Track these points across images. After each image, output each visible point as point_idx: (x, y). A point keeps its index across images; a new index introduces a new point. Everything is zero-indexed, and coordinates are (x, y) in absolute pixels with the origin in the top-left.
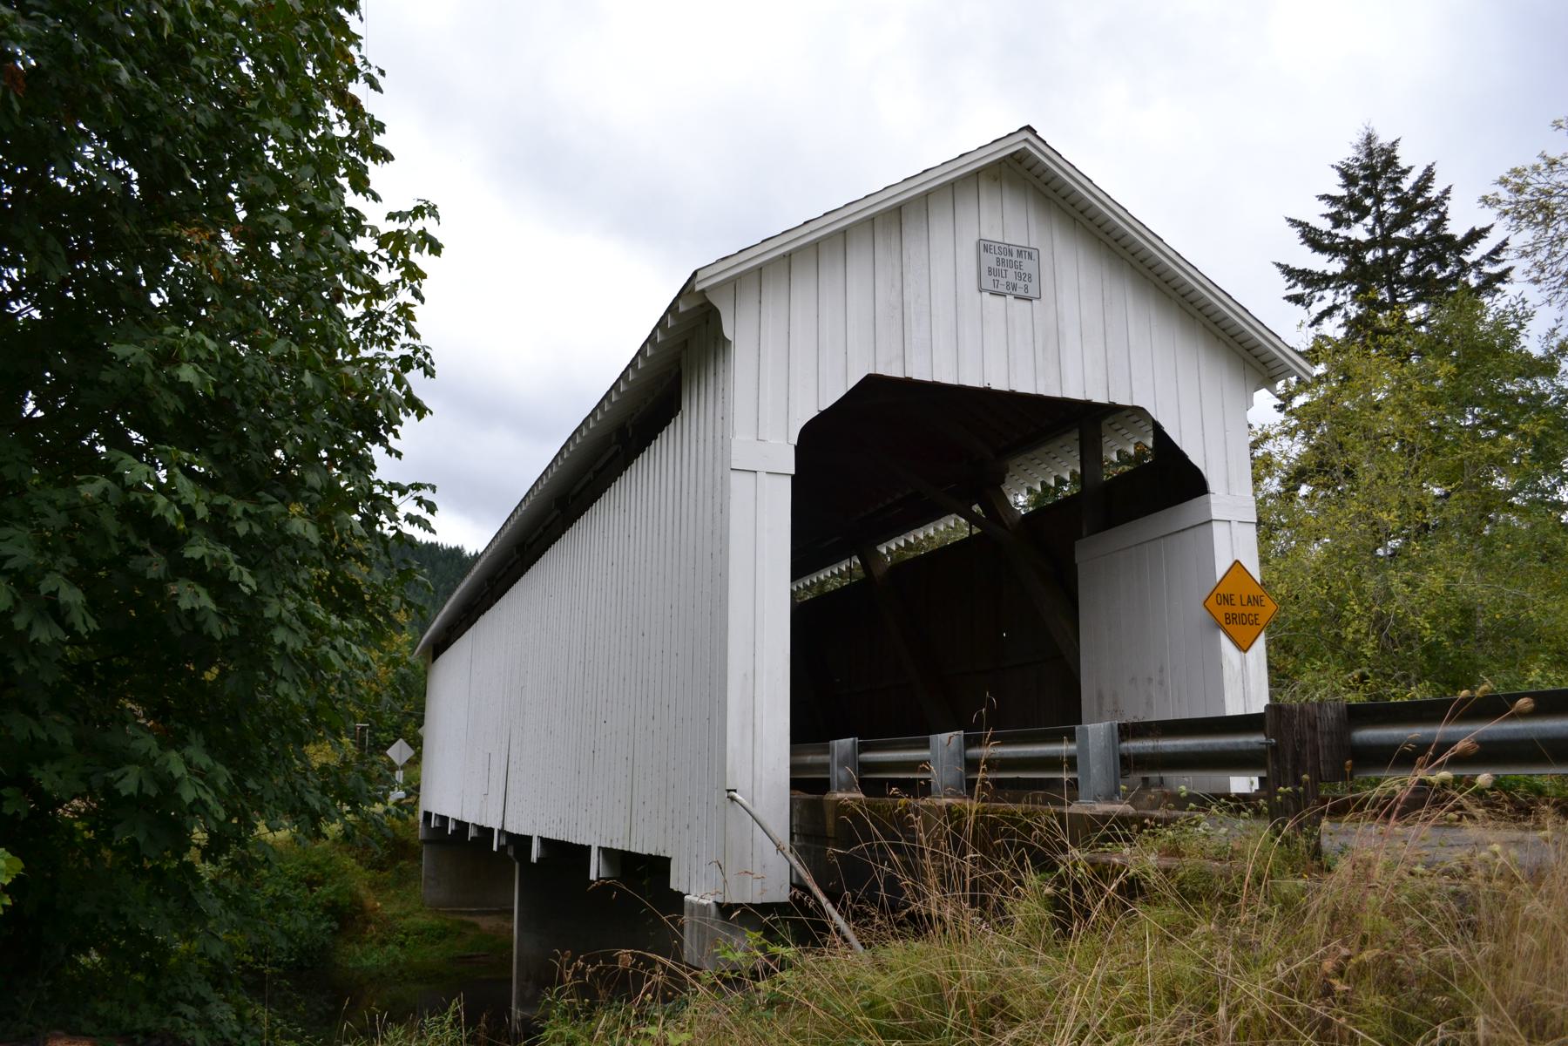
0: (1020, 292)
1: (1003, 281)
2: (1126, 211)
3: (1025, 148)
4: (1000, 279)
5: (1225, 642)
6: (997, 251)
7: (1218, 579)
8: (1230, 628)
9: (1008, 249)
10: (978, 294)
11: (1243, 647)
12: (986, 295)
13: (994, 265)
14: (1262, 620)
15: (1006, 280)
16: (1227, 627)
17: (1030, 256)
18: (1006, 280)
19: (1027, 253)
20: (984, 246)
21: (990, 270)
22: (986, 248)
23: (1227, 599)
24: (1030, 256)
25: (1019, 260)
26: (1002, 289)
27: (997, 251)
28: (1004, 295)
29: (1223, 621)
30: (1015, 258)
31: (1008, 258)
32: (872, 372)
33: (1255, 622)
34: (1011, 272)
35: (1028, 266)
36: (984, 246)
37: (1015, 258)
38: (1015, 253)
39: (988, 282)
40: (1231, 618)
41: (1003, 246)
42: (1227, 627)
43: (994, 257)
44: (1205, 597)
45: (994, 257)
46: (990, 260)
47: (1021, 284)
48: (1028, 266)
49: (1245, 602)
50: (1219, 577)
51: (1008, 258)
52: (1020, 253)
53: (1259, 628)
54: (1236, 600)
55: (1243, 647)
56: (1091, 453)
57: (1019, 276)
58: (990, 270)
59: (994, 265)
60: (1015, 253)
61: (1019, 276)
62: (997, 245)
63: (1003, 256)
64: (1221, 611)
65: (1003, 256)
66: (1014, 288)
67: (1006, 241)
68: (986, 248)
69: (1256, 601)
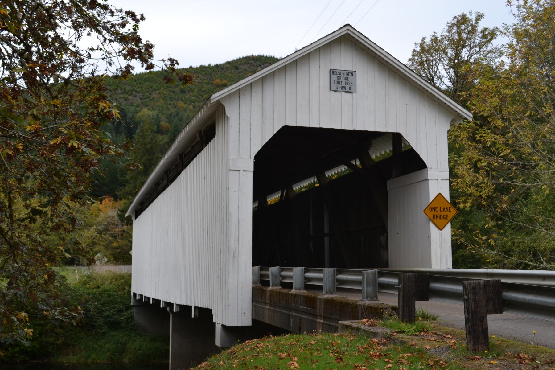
0: (347, 90)
1: (340, 86)
2: (391, 55)
3: (347, 33)
4: (339, 85)
5: (432, 226)
6: (338, 73)
7: (430, 201)
8: (434, 220)
9: (342, 72)
10: (330, 92)
11: (441, 228)
12: (333, 92)
13: (336, 80)
14: (450, 217)
15: (341, 85)
16: (434, 220)
17: (352, 75)
18: (341, 85)
19: (352, 73)
20: (333, 72)
21: (335, 82)
22: (333, 73)
23: (434, 209)
24: (352, 75)
25: (347, 76)
26: (340, 89)
27: (338, 73)
28: (340, 92)
29: (432, 218)
30: (345, 76)
31: (342, 76)
32: (284, 125)
33: (446, 218)
34: (344, 82)
35: (351, 79)
36: (333, 72)
37: (345, 76)
38: (345, 74)
39: (334, 87)
40: (435, 217)
41: (340, 71)
42: (434, 220)
43: (336, 76)
44: (424, 209)
45: (336, 76)
46: (335, 78)
47: (348, 87)
48: (351, 79)
49: (442, 210)
50: (431, 201)
51: (342, 76)
52: (347, 74)
53: (448, 220)
54: (438, 209)
55: (441, 228)
56: (365, 157)
57: (347, 83)
58: (335, 82)
59: (336, 80)
60: (345, 74)
61: (347, 83)
62: (338, 71)
63: (340, 76)
64: (431, 214)
65: (340, 76)
66: (345, 88)
67: (342, 69)
68: (333, 73)
69: (448, 209)
